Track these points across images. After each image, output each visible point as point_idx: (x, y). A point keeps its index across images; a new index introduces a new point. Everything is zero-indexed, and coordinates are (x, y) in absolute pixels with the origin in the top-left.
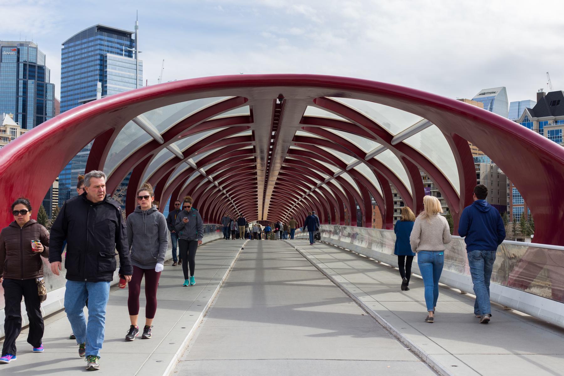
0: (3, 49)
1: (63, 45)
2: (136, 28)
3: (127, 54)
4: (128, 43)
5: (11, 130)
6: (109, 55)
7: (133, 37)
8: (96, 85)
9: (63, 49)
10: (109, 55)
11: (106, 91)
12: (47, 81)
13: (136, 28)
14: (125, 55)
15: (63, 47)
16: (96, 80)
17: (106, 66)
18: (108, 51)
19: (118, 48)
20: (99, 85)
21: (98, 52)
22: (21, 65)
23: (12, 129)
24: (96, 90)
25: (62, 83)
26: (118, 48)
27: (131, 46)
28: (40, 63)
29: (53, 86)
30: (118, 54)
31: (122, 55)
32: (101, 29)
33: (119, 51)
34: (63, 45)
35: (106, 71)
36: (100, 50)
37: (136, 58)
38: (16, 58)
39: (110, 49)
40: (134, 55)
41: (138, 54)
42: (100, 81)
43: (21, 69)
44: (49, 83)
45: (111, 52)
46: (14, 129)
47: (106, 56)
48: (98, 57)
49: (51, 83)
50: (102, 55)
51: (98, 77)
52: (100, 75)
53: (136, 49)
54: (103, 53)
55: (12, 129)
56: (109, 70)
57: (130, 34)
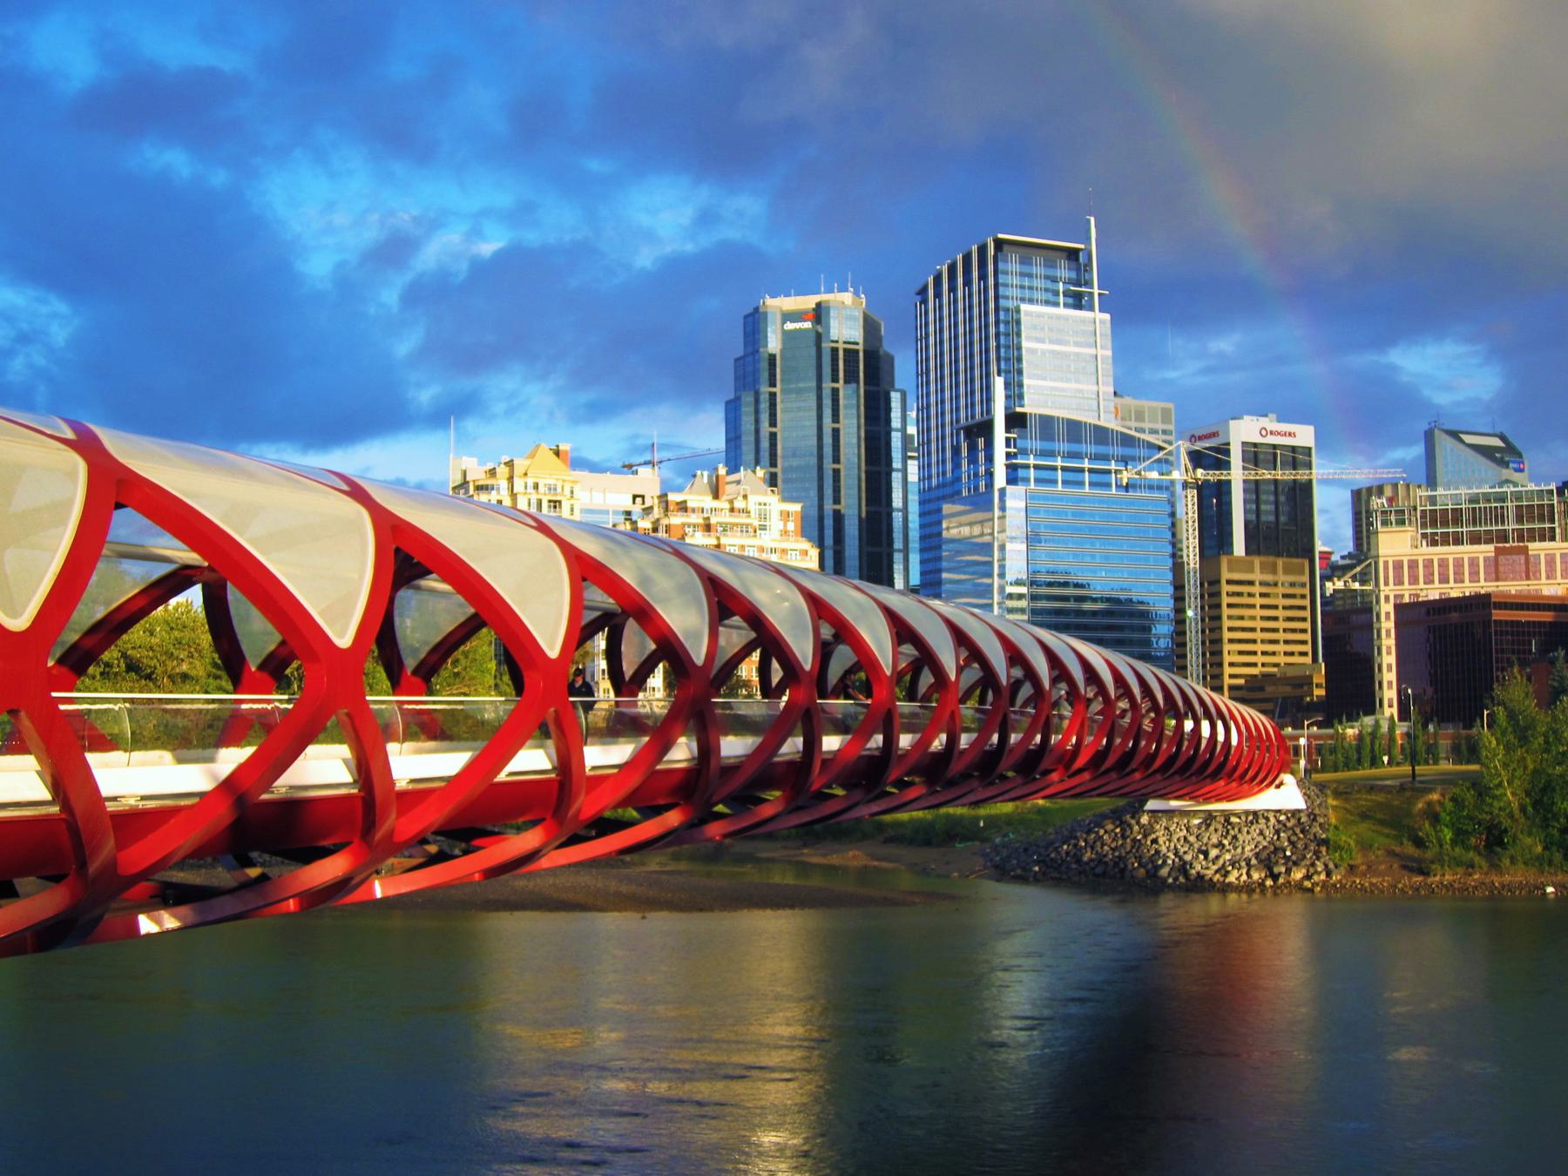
3: (1070, 301)
5: (758, 507)
6: (1024, 307)
10: (1024, 307)
14: (1066, 305)
18: (1023, 300)
19: (1046, 290)
23: (760, 504)
26: (1046, 290)
30: (1047, 303)
31: (1056, 304)
33: (1050, 297)
39: (1027, 293)
45: (1031, 301)
46: (765, 504)
47: (1018, 311)
55: (760, 504)
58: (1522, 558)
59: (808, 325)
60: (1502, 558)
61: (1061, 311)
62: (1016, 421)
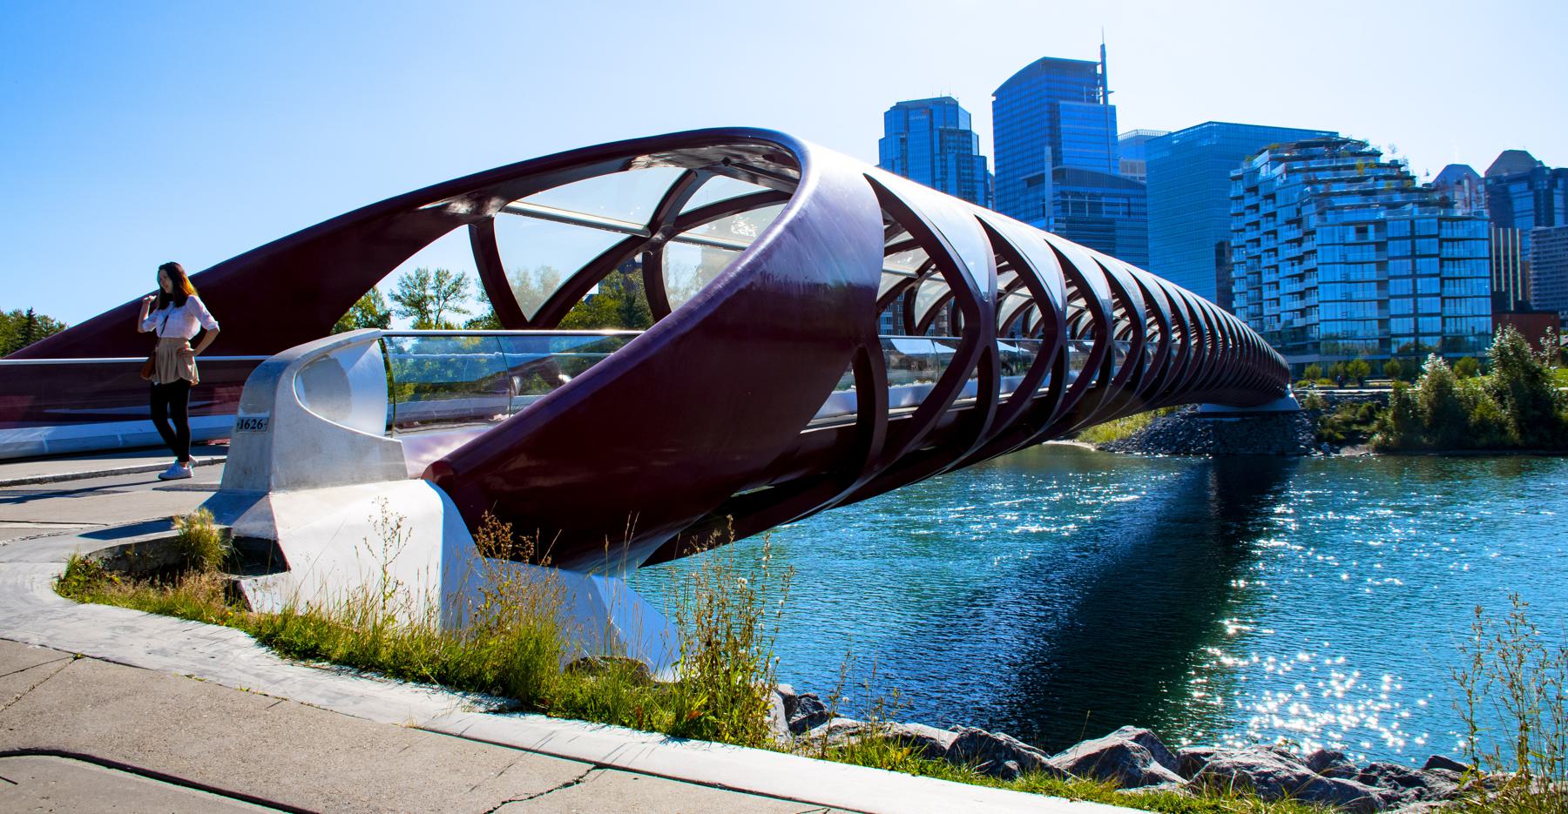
0: (910, 113)
1: (993, 95)
7: (1099, 71)
8: (1043, 152)
9: (993, 102)
10: (1061, 102)
11: (1061, 159)
12: (975, 154)
15: (994, 99)
16: (1042, 145)
17: (1059, 120)
20: (1048, 150)
22: (936, 134)
24: (1043, 160)
25: (995, 154)
27: (1097, 86)
28: (963, 126)
29: (984, 158)
31: (1082, 100)
34: (993, 95)
35: (1059, 129)
36: (1049, 96)
38: (928, 124)
41: (1109, 96)
42: (1051, 144)
43: (937, 140)
44: (978, 156)
45: (1066, 98)
47: (1059, 105)
49: (980, 154)
53: (1104, 85)
56: (1064, 126)
57: (1094, 65)
59: (924, 117)
61: (1085, 104)
62: (1058, 174)
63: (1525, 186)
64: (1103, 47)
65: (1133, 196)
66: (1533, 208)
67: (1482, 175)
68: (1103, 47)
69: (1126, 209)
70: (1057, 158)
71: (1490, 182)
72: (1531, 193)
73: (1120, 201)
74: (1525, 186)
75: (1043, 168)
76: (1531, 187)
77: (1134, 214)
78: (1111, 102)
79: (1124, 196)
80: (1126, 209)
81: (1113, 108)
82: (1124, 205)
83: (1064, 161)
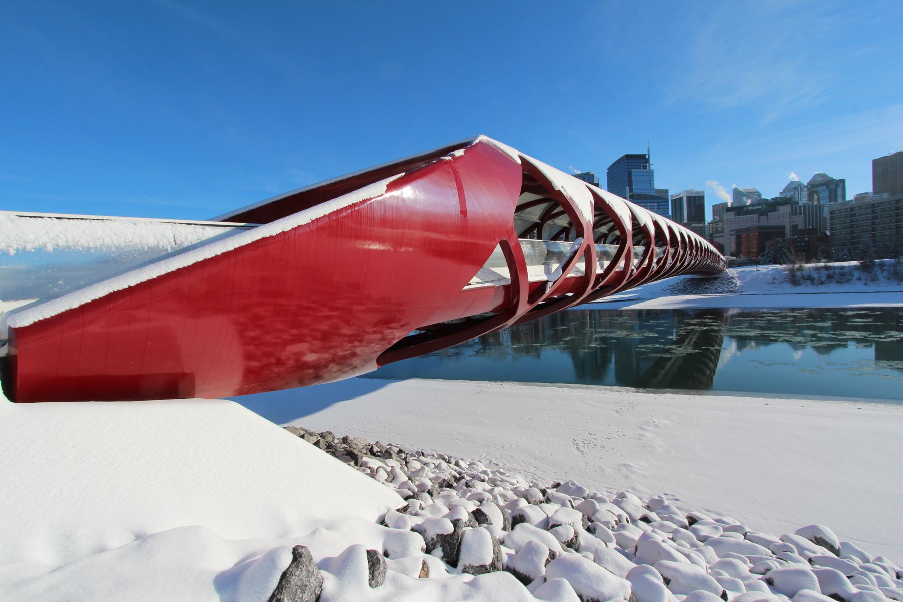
2: (649, 151)
4: (644, 161)
7: (647, 157)
8: (625, 189)
9: (607, 172)
10: (633, 170)
13: (649, 151)
20: (627, 188)
21: (626, 170)
27: (646, 163)
30: (638, 168)
31: (640, 168)
32: (628, 157)
33: (638, 167)
37: (649, 168)
39: (633, 167)
40: (648, 168)
42: (629, 185)
47: (631, 171)
48: (627, 172)
50: (628, 171)
51: (627, 184)
52: (628, 182)
53: (649, 163)
54: (629, 169)
56: (633, 178)
57: (645, 155)
58: (765, 217)
60: (760, 217)
61: (642, 170)
63: (825, 187)
64: (648, 148)
65: (661, 202)
66: (828, 195)
67: (806, 184)
68: (648, 148)
69: (657, 207)
70: (631, 190)
71: (809, 186)
72: (828, 190)
73: (655, 204)
74: (825, 187)
75: (626, 194)
76: (827, 187)
77: (661, 208)
78: (651, 168)
79: (657, 202)
80: (657, 207)
81: (653, 170)
82: (657, 206)
83: (634, 191)
